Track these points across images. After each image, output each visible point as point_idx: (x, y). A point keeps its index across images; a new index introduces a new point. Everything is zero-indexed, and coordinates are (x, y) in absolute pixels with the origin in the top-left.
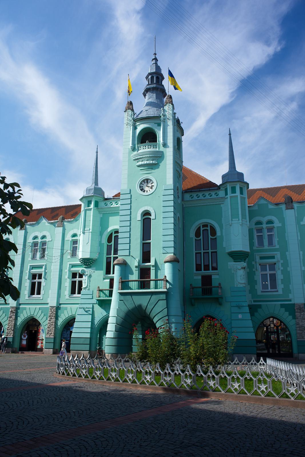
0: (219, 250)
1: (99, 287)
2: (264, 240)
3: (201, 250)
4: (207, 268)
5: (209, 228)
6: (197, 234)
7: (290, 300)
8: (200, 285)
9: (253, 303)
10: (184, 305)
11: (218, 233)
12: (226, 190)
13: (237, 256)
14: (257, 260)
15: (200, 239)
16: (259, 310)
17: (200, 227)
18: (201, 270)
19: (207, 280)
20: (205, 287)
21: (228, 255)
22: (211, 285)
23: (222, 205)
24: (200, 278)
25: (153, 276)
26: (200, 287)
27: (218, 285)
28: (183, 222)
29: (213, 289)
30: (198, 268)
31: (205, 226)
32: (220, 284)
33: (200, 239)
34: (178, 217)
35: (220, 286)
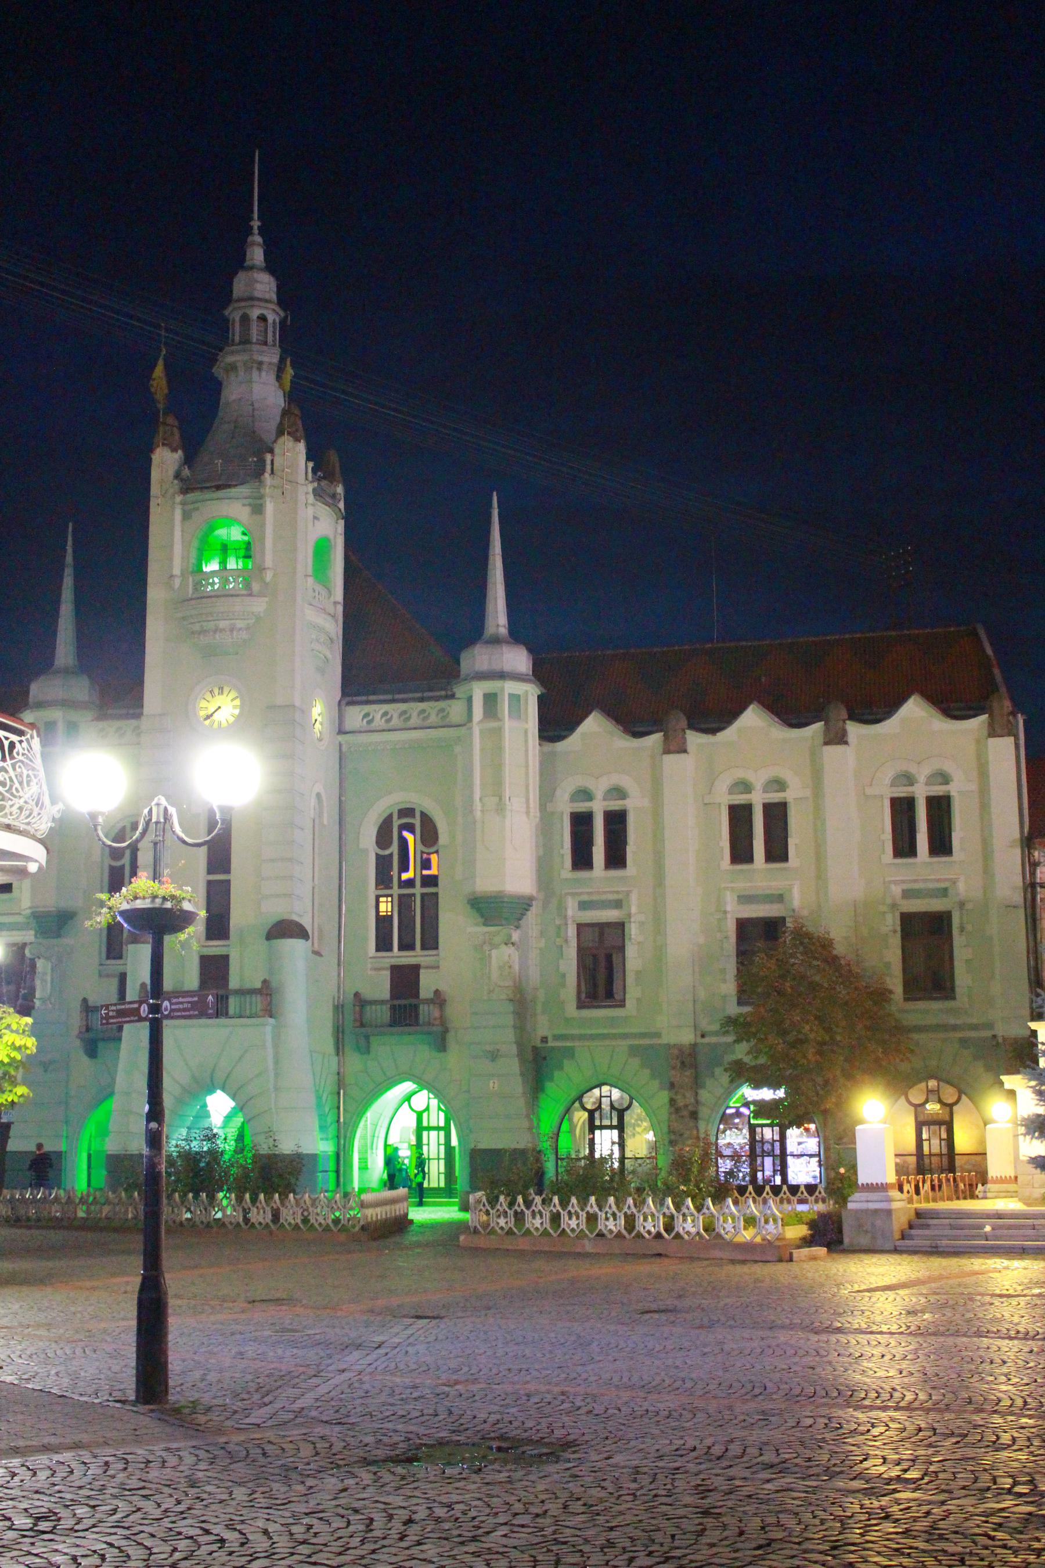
0: (443, 890)
1: (85, 1000)
2: (594, 849)
3: (391, 888)
4: (406, 945)
5: (417, 822)
6: (383, 836)
7: (658, 1035)
8: (386, 995)
9: (551, 1044)
10: (338, 1054)
11: (443, 839)
12: (470, 700)
13: (494, 910)
14: (570, 913)
15: (391, 855)
16: (566, 1062)
17: (390, 816)
18: (390, 949)
19: (405, 980)
20: (403, 1002)
21: (469, 907)
22: (417, 995)
23: (458, 749)
24: (388, 973)
25: (234, 983)
26: (382, 1002)
27: (431, 996)
28: (340, 801)
29: (423, 1009)
30: (383, 943)
31: (407, 812)
32: (437, 992)
33: (391, 855)
34: (318, 795)
35: (439, 999)
